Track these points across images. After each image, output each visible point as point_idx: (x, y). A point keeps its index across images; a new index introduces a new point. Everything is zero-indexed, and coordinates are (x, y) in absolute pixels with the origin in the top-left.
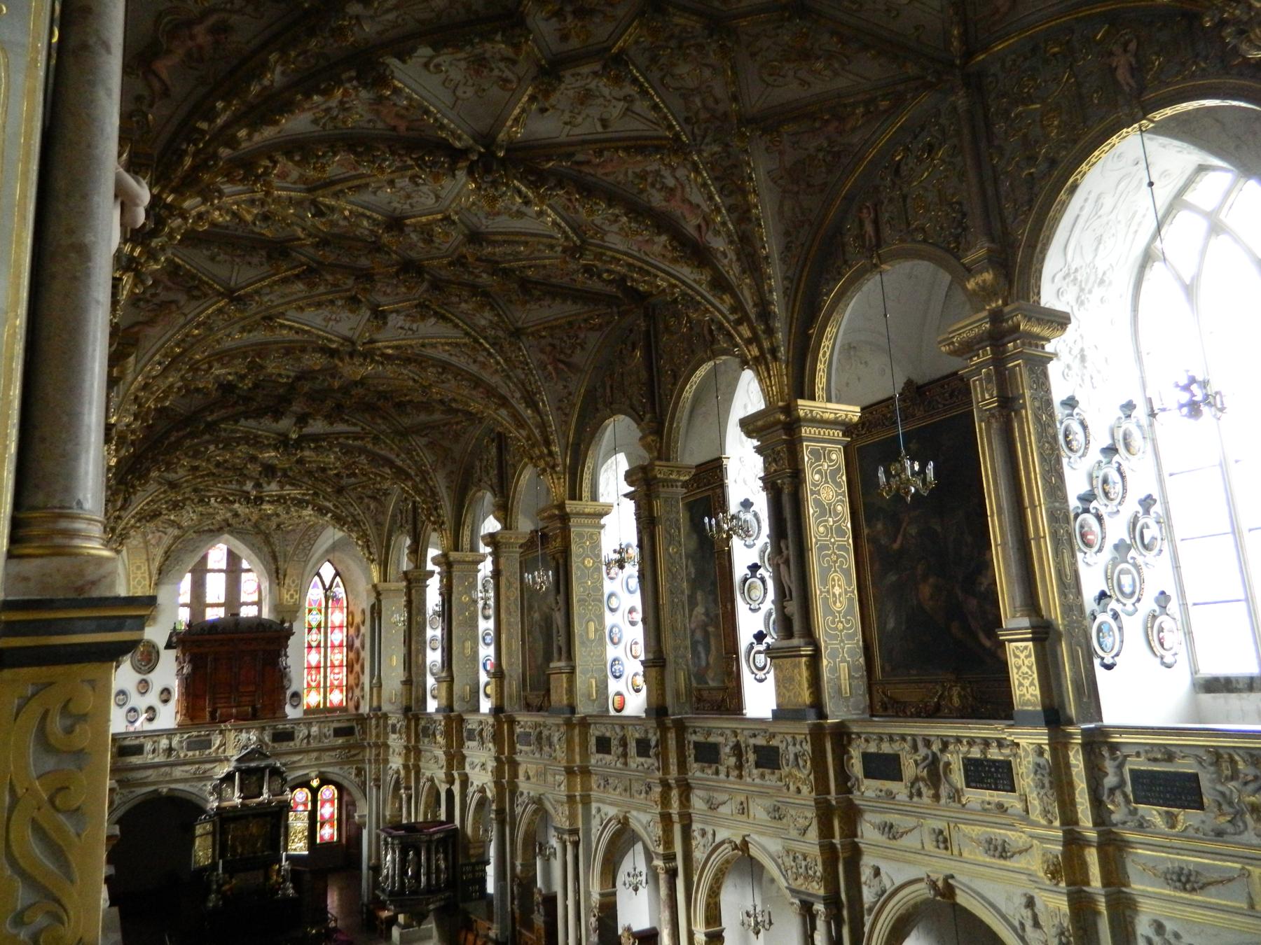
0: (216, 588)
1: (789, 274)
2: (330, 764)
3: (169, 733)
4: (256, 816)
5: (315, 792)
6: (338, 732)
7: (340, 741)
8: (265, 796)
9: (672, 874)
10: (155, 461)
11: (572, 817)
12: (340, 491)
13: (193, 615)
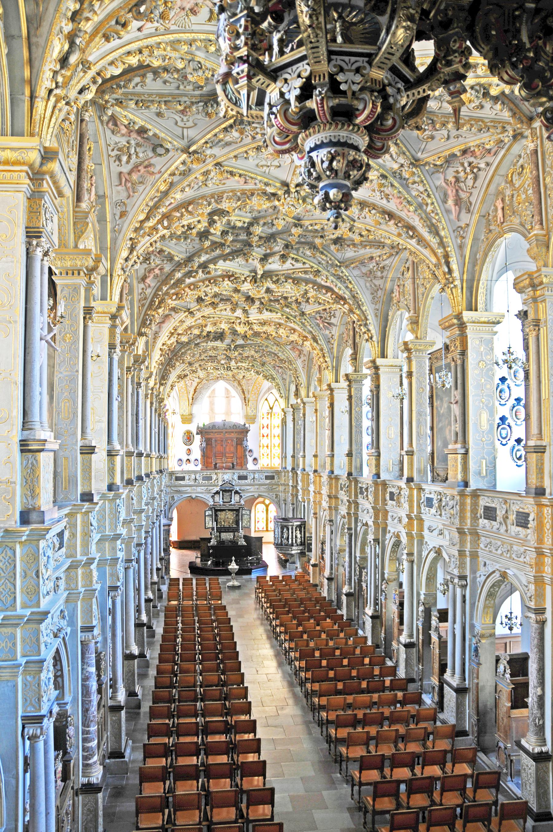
1: (377, 307)
2: (264, 492)
3: (195, 472)
4: (229, 510)
5: (267, 506)
6: (267, 478)
7: (268, 481)
8: (232, 503)
9: (351, 535)
10: (177, 360)
11: (331, 515)
12: (263, 365)
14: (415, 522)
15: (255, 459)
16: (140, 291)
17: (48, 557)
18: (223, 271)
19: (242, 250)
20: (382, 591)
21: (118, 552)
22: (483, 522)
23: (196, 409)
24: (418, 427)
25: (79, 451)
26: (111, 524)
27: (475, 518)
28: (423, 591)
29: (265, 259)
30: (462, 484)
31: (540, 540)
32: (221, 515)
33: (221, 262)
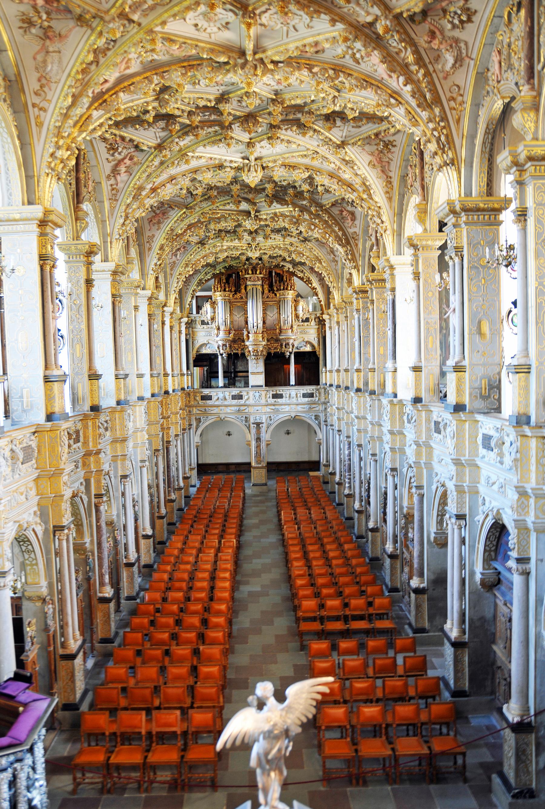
7: (306, 399)
14: (424, 450)
22: (482, 451)
24: (426, 338)
28: (433, 529)
31: (524, 477)
33: (201, 149)
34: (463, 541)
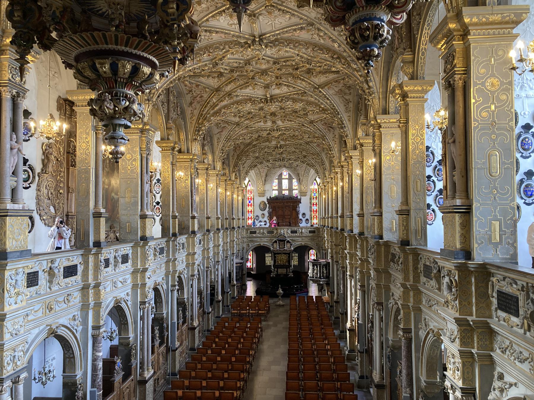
0: (285, 184)
7: (312, 234)
13: (279, 193)
15: (307, 220)
16: (190, 112)
17: (16, 280)
18: (242, 96)
19: (250, 81)
20: (356, 312)
21: (147, 280)
23: (267, 187)
25: (91, 216)
26: (141, 262)
27: (387, 262)
29: (267, 87)
30: (378, 237)
32: (279, 257)
34: (381, 319)
